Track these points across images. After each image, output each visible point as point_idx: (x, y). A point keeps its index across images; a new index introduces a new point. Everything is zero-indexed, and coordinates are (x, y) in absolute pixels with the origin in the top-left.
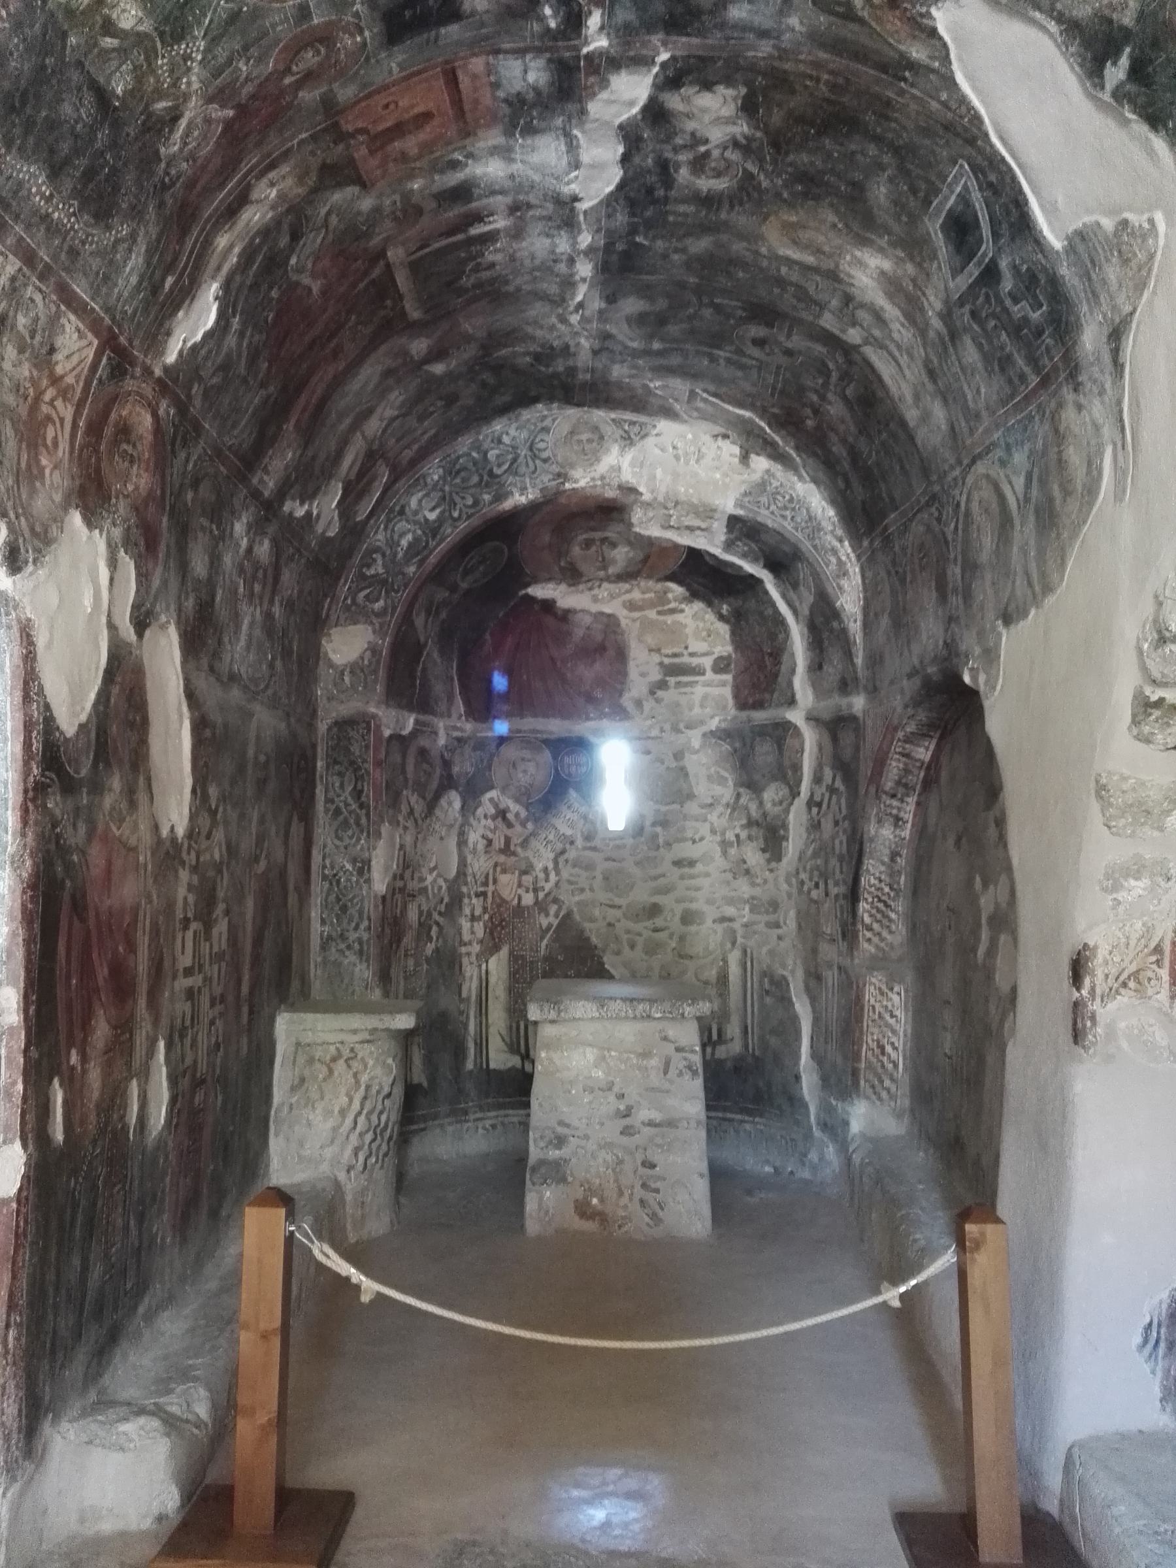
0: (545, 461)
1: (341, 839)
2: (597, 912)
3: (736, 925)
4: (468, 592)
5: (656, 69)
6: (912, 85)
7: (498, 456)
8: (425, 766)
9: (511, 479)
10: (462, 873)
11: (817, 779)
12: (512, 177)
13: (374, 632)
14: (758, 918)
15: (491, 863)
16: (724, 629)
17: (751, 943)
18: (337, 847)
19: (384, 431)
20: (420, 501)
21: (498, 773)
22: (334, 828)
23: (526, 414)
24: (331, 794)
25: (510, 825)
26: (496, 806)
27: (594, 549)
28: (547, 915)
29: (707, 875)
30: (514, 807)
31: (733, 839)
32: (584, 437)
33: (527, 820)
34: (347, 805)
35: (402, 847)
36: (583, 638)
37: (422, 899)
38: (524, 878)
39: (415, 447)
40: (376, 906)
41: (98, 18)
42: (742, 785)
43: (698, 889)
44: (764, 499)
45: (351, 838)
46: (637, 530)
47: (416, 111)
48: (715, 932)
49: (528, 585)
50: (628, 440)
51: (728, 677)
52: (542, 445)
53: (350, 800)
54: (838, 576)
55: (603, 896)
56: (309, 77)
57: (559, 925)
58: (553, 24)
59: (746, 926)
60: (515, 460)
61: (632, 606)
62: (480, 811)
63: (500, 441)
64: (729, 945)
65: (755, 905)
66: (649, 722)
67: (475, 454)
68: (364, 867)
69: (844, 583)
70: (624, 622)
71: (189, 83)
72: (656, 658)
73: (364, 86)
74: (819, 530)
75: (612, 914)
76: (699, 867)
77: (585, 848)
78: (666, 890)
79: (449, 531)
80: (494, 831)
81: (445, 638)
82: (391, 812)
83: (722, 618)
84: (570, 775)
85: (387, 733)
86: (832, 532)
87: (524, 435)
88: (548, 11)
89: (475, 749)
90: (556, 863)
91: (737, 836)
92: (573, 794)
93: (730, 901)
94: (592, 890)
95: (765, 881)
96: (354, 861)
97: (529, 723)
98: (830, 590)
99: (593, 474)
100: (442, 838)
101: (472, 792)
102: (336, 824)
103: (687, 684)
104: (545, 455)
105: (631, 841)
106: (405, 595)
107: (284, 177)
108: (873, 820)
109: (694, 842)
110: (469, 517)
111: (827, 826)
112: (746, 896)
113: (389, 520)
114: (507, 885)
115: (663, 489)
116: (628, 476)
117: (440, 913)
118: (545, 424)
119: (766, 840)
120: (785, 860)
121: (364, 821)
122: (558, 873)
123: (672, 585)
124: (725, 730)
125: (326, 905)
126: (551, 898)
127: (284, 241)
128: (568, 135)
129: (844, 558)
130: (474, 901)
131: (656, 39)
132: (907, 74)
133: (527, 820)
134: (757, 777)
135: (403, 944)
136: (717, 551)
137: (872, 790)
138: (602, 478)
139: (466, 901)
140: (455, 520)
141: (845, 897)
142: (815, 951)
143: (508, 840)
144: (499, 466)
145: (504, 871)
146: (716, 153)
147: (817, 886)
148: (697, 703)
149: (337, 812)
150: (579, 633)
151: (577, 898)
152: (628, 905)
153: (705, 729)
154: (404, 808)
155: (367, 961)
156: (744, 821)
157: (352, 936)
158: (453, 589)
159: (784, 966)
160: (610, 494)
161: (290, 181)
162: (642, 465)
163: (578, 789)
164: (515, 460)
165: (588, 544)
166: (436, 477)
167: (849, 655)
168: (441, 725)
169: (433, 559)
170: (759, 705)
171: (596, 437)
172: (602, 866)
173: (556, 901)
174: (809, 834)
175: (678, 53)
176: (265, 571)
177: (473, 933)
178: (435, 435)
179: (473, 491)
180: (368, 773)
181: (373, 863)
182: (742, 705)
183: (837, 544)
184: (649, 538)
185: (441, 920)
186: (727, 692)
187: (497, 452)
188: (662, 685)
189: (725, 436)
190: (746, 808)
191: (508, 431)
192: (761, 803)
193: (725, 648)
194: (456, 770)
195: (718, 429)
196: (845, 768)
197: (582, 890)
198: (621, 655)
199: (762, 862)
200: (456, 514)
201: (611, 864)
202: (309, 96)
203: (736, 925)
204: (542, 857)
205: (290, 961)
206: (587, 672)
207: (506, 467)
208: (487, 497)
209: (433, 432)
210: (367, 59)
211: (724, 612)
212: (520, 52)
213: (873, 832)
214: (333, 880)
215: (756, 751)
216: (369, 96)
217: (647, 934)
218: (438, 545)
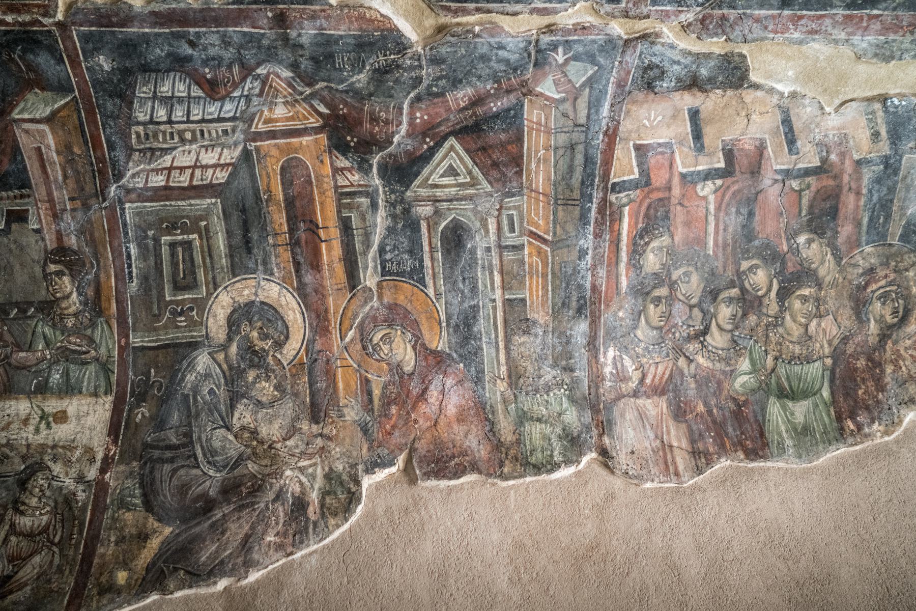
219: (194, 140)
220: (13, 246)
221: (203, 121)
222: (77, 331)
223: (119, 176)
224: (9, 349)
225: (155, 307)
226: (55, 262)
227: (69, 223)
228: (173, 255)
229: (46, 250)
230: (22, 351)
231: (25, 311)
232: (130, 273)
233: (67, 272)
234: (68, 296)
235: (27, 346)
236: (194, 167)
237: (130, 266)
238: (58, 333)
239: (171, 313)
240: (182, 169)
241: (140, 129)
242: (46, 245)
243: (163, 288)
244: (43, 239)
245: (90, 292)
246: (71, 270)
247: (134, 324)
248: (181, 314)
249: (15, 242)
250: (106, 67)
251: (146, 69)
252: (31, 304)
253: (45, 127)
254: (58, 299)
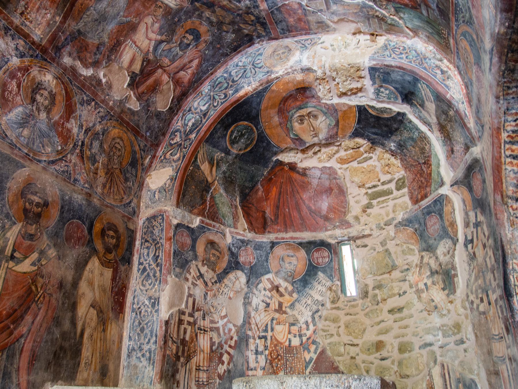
0: (260, 68)
1: (143, 285)
2: (342, 349)
3: (435, 348)
4: (237, 156)
7: (236, 72)
8: (214, 251)
9: (243, 80)
10: (247, 321)
11: (467, 225)
13: (173, 170)
14: (448, 340)
15: (268, 319)
16: (397, 162)
17: (447, 360)
18: (141, 290)
19: (155, 48)
20: (199, 103)
21: (273, 263)
22: (142, 279)
23: (251, 50)
24: (142, 260)
25: (282, 295)
26: (272, 283)
27: (306, 122)
28: (309, 352)
29: (411, 316)
30: (284, 285)
31: (423, 287)
32: (280, 52)
33: (293, 291)
34: (149, 265)
35: (190, 295)
36: (318, 185)
37: (214, 335)
38: (292, 328)
39: (190, 71)
40: (161, 327)
42: (424, 250)
43: (406, 327)
44: (387, 53)
45: (150, 285)
46: (324, 101)
48: (422, 356)
49: (276, 154)
50: (304, 47)
51: (406, 190)
52: (258, 62)
53: (152, 262)
54: (444, 80)
55: (346, 339)
57: (318, 358)
59: (441, 347)
60: (245, 71)
61: (342, 161)
62: (261, 286)
63: (237, 66)
64: (432, 364)
65: (444, 330)
66: (364, 227)
67: (225, 75)
68: (155, 302)
69: (449, 83)
70: (339, 172)
72: (364, 191)
74: (425, 59)
75: (353, 351)
76: (405, 312)
77: (332, 309)
78: (386, 331)
79: (212, 113)
80: (271, 298)
81: (229, 182)
82: (177, 270)
83: (393, 154)
84: (318, 264)
85: (175, 222)
86: (434, 57)
87: (250, 59)
89: (255, 249)
90: (313, 318)
91: (425, 284)
92: (321, 275)
93: (428, 331)
94: (339, 335)
95: (449, 311)
96: (150, 298)
97: (290, 234)
98: (440, 89)
99: (286, 67)
100: (230, 298)
101: (254, 273)
102: (143, 276)
103: (383, 202)
104: (259, 66)
105: (361, 301)
106: (192, 148)
108: (507, 225)
109: (400, 295)
110: (222, 103)
111: (480, 252)
112: (438, 325)
113: (184, 115)
114: (281, 333)
115: (327, 66)
116: (306, 63)
117: (230, 346)
118: (260, 52)
119: (444, 282)
120: (458, 291)
121: (158, 274)
122: (314, 325)
123: (360, 141)
124: (407, 220)
125: (132, 328)
126: (310, 341)
129: (445, 69)
130: (258, 341)
133: (293, 291)
134: (431, 242)
135: (194, 360)
136: (374, 103)
137: (499, 198)
138: (291, 67)
139: (251, 341)
140: (215, 107)
141: (501, 297)
142: (490, 352)
143: (280, 304)
144: (237, 76)
145: (279, 323)
147: (482, 300)
148: (391, 211)
149: (145, 270)
150: (315, 182)
151: (328, 341)
152: (363, 343)
153: (395, 222)
154: (193, 272)
155: (153, 364)
156: (429, 273)
157: (146, 347)
158: (227, 152)
159: (471, 371)
160: (299, 77)
162: (314, 57)
163: (324, 271)
164: (245, 71)
165: (301, 119)
166: (207, 91)
167: (464, 126)
168: (227, 230)
169: (204, 129)
170: (425, 196)
171: (286, 51)
172: (344, 319)
173: (314, 342)
174: (470, 265)
176: (53, 97)
177: (257, 362)
178: (200, 65)
179: (224, 91)
180: (162, 245)
181: (161, 300)
182: (416, 201)
183: (438, 63)
184: (332, 105)
185: (232, 351)
186: (407, 199)
187: (236, 70)
188: (369, 206)
189: (360, 32)
190: (428, 264)
191: (241, 60)
192: (437, 258)
193: (400, 173)
194: (241, 259)
195: (353, 27)
196: (480, 204)
197: (332, 335)
198: (342, 192)
199: (444, 297)
200: (215, 104)
201: (349, 317)
203: (435, 348)
204: (304, 315)
205: (77, 352)
206: (324, 204)
207: (240, 76)
208: (231, 92)
209: (196, 62)
211: (393, 148)
213: (509, 236)
214: (138, 312)
215: (427, 223)
217: (377, 362)
218: (207, 121)
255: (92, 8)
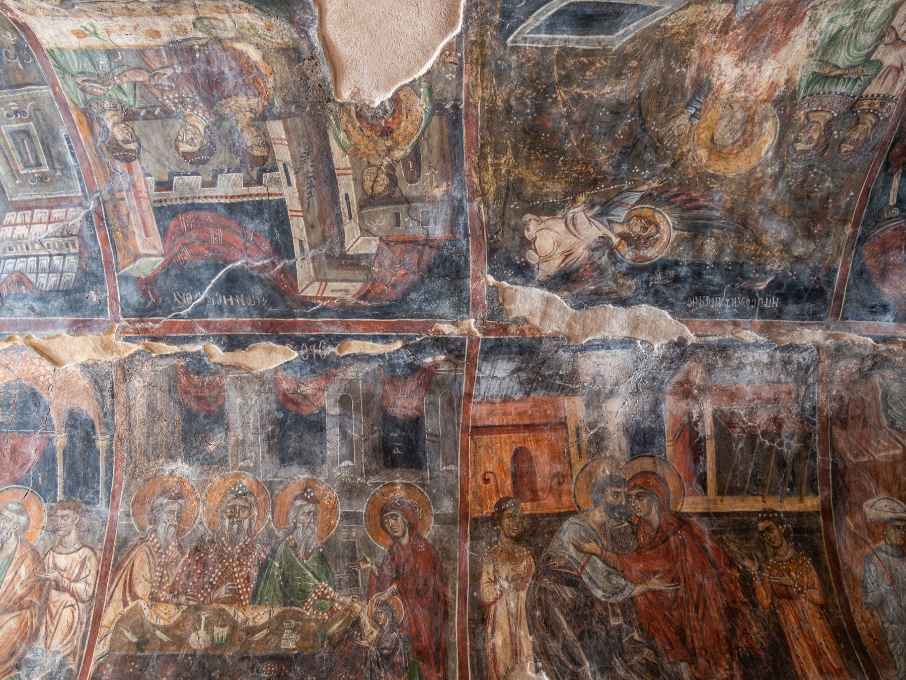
5: (505, 284)
6: (457, 99)
12: (636, 393)
41: (241, 633)
47: (507, 459)
56: (413, 527)
58: (443, 357)
71: (341, 603)
73: (451, 493)
88: (429, 360)
107: (495, 571)
127: (568, 593)
128: (584, 349)
131: (471, 284)
132: (448, 106)
146: (619, 229)
161: (505, 570)
175: (487, 268)
202: (431, 530)
210: (423, 486)
212: (472, 379)
216: (464, 493)
219: (33, 243)
220: (167, 163)
221: (27, 257)
222: (98, 98)
223: (88, 217)
224: (153, 83)
225: (40, 116)
226: (131, 150)
227: (123, 181)
228: (37, 158)
229: (139, 159)
230: (142, 82)
231: (148, 112)
232: (69, 142)
233: (120, 143)
234: (115, 124)
235: (137, 86)
236: (31, 223)
237: (71, 147)
238: (114, 96)
239: (25, 112)
240: (40, 223)
241: (72, 250)
242: (140, 163)
243: (38, 131)
244: (143, 168)
245: (97, 128)
246: (118, 145)
247: (53, 103)
248: (16, 112)
249: (164, 166)
250: (92, 293)
251: (67, 292)
252: (145, 118)
253: (142, 251)
254: (123, 122)
255: (886, 625)
